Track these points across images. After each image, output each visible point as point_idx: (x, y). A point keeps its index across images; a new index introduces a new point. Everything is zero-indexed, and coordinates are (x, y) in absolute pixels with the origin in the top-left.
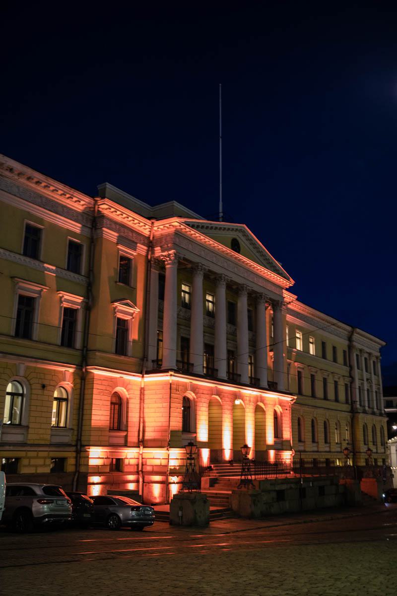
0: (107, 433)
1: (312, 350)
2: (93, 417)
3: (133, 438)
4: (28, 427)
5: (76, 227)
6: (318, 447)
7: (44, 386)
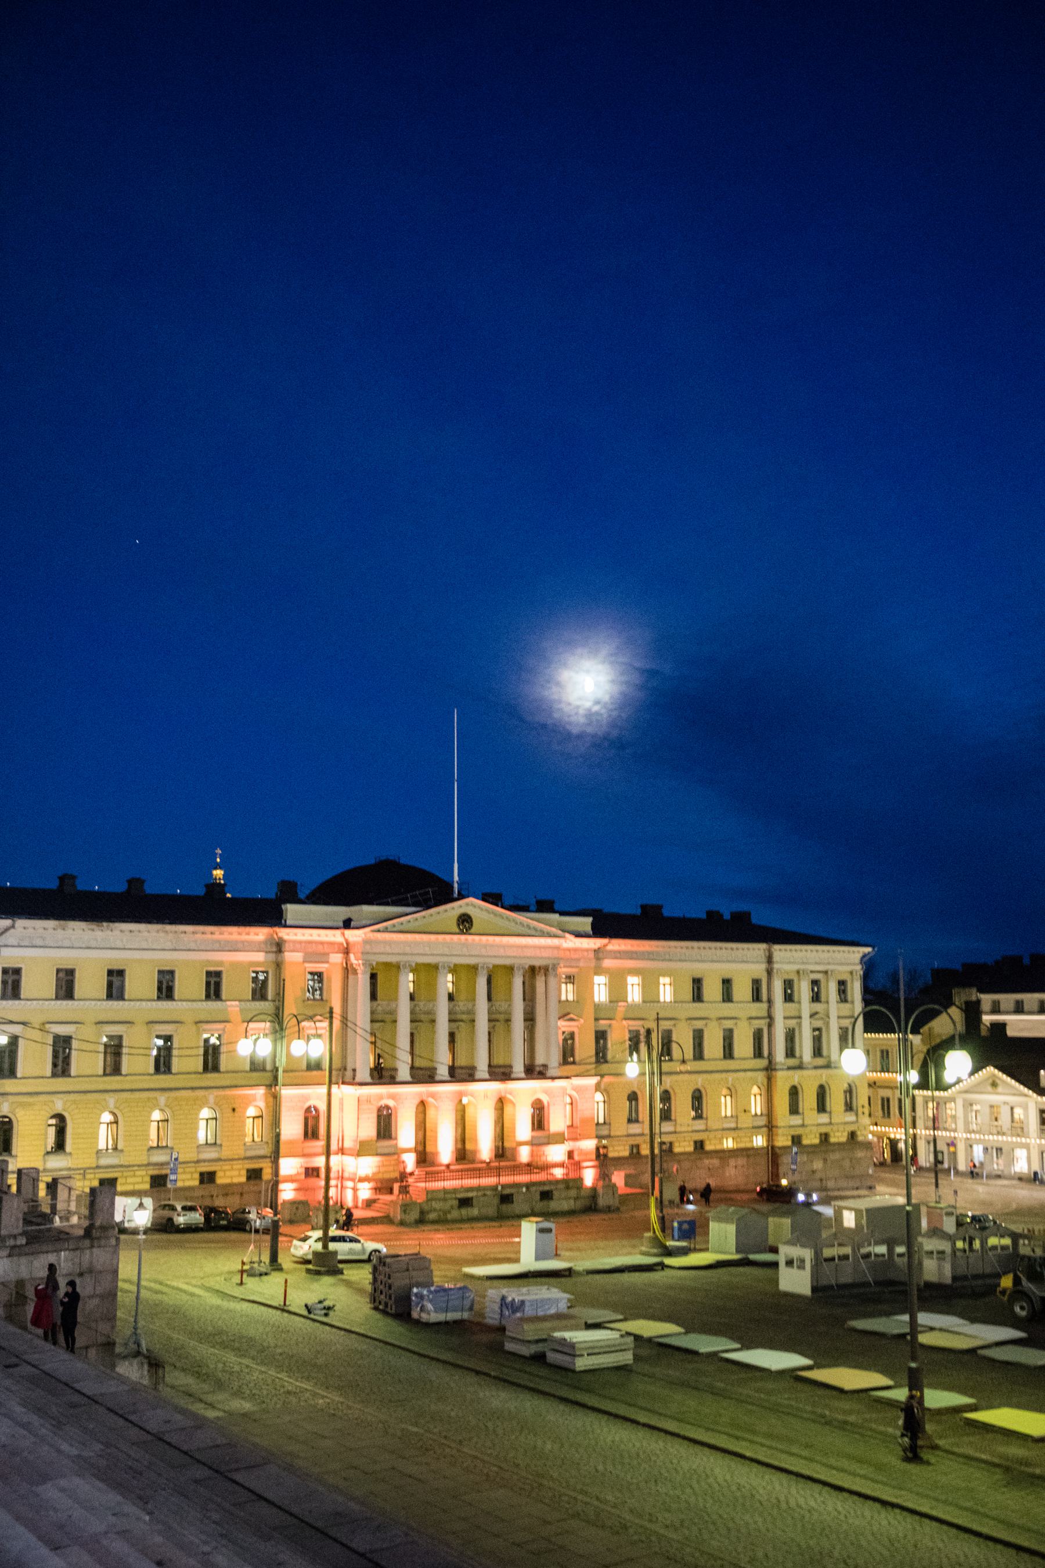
1: (666, 993)
4: (221, 1145)
5: (260, 957)
6: (675, 1125)
7: (234, 1110)
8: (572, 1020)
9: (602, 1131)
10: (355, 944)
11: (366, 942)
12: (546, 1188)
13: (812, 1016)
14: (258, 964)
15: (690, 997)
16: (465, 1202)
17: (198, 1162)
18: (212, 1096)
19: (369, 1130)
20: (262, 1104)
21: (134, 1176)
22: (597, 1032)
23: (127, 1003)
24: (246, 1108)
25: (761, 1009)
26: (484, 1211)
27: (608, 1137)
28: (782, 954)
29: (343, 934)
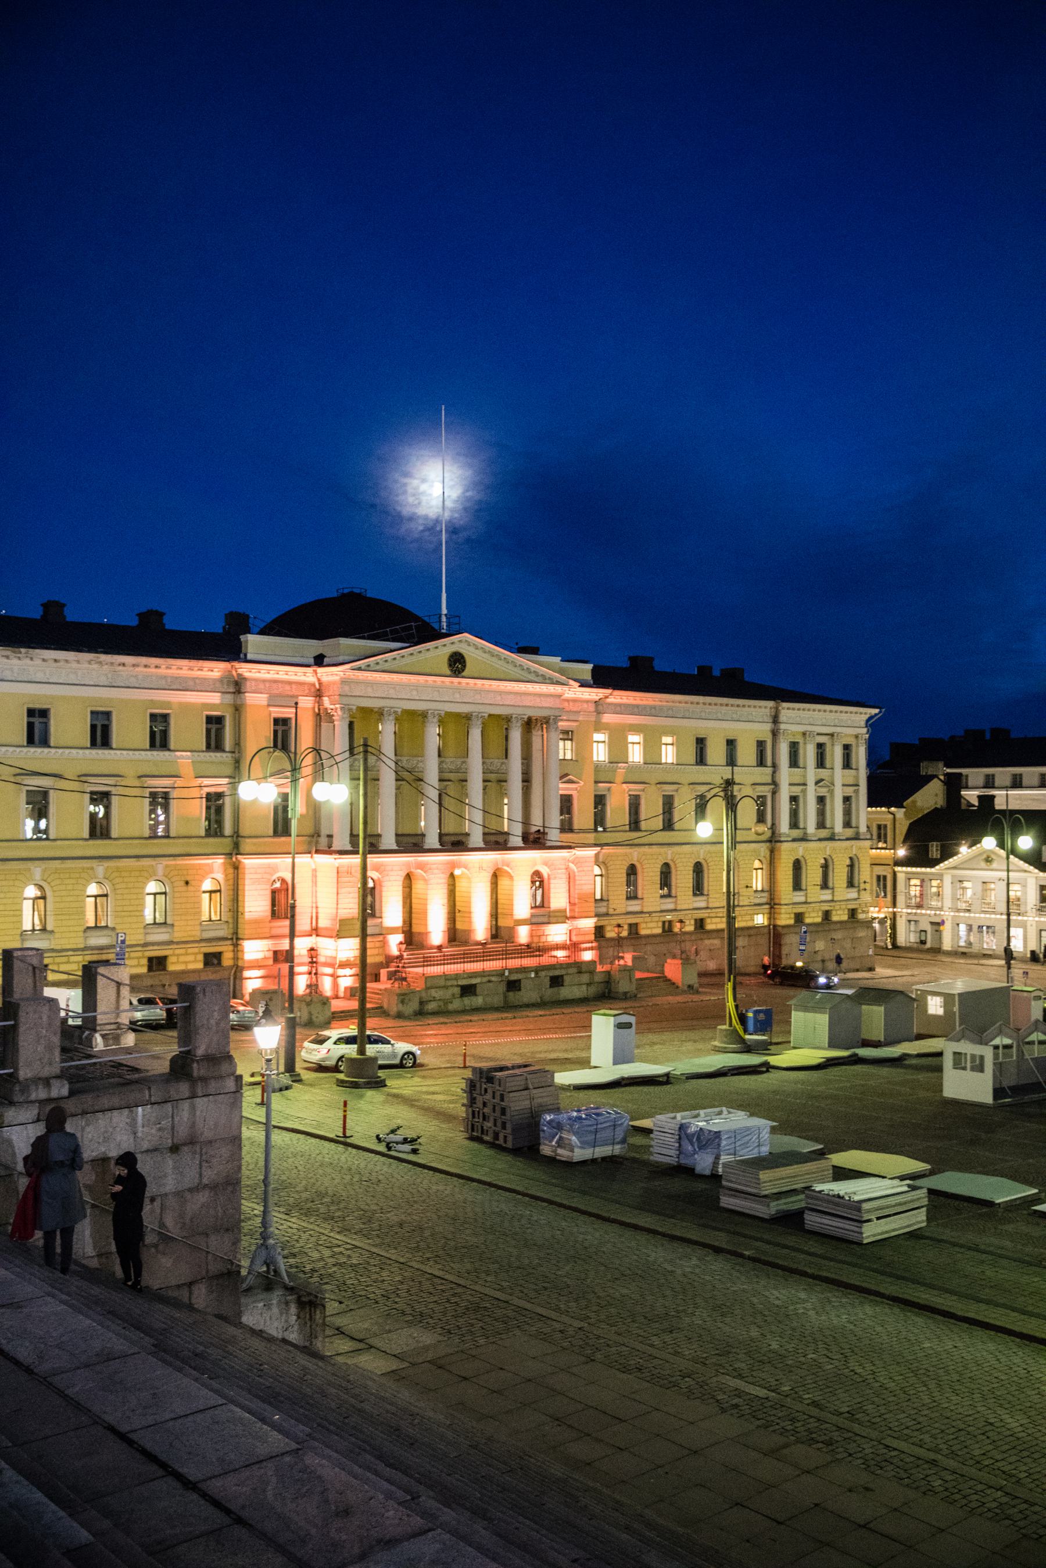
0: (268, 925)
1: (669, 755)
2: (247, 909)
5: (215, 698)
6: (676, 903)
7: (187, 883)
9: (601, 906)
10: (330, 683)
11: (344, 682)
12: (557, 973)
13: (817, 783)
14: (212, 706)
15: (693, 760)
16: (468, 990)
17: (145, 945)
18: (160, 865)
19: (350, 906)
20: (220, 876)
21: (68, 962)
22: (596, 796)
23: (53, 751)
24: (201, 881)
25: (764, 774)
26: (489, 1000)
27: (607, 914)
28: (790, 713)
29: (315, 672)
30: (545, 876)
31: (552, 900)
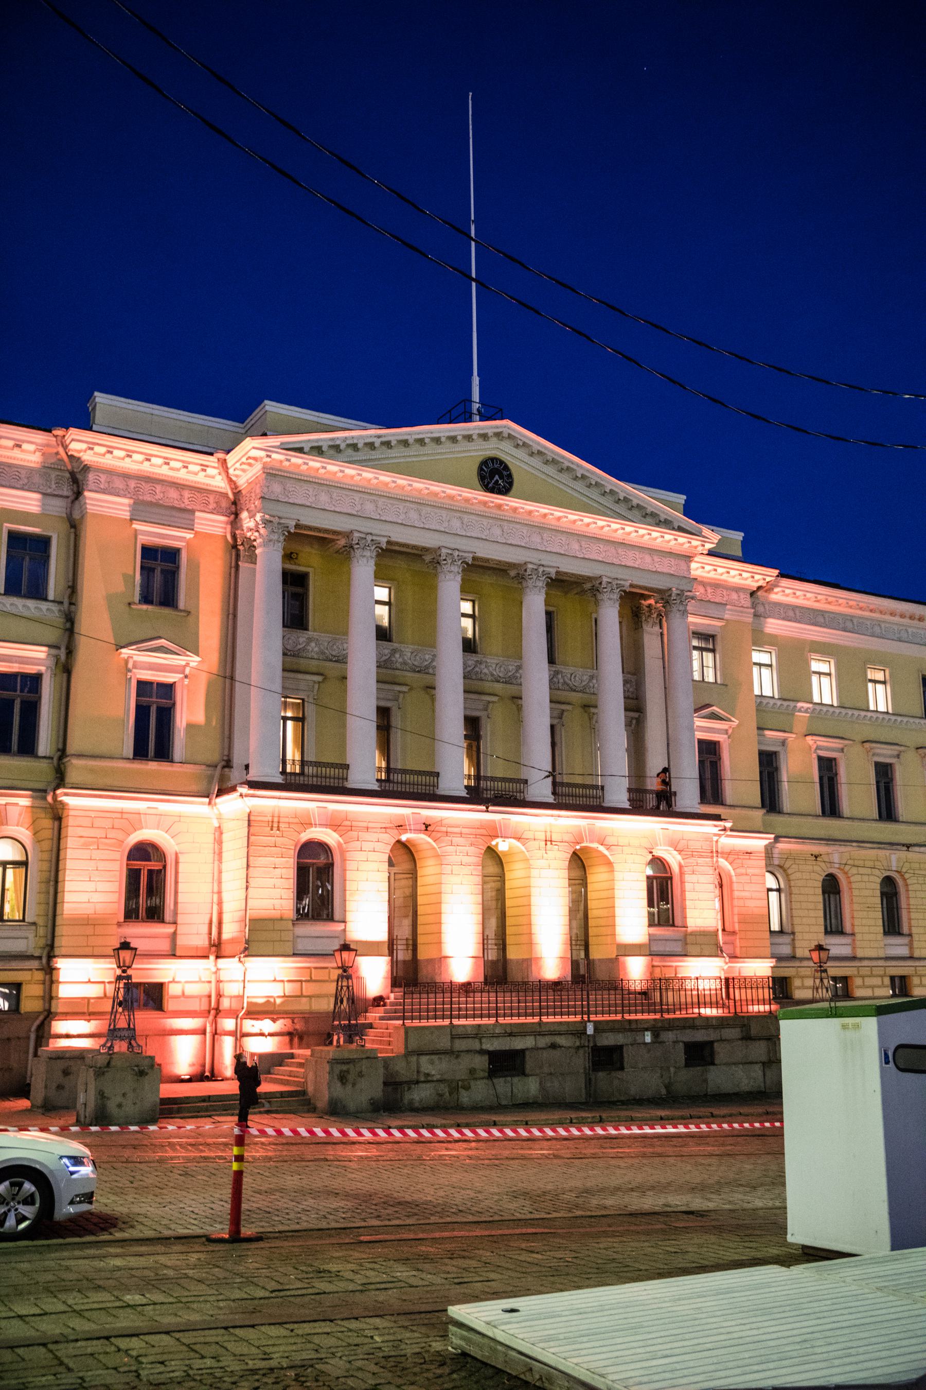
1: (880, 699)
3: (194, 933)
5: (28, 502)
6: (911, 946)
8: (714, 716)
12: (700, 1036)
14: (25, 517)
16: (506, 1063)
19: (276, 893)
20: (25, 834)
22: (762, 754)
26: (554, 1086)
30: (675, 868)
31: (689, 913)
